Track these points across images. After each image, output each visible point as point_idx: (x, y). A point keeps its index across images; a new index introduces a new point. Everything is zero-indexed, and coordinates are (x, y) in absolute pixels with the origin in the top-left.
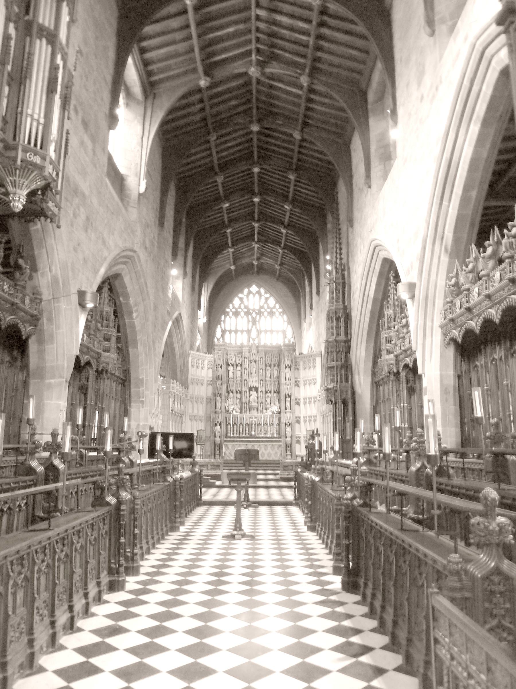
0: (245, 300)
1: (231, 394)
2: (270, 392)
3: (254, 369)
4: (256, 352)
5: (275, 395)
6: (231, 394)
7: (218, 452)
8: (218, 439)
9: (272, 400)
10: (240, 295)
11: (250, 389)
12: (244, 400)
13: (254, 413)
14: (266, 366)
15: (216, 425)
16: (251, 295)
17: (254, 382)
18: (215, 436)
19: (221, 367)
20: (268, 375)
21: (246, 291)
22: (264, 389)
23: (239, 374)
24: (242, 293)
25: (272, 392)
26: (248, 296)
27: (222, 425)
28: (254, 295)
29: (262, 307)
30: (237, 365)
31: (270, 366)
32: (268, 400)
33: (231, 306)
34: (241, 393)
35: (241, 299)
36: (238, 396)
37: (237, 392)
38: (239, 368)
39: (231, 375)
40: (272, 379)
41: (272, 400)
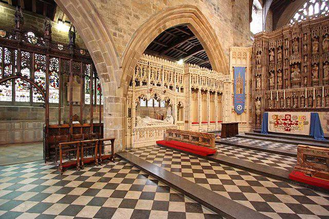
0: (305, 13)
1: (273, 75)
2: (318, 65)
3: (297, 47)
4: (298, 31)
5: (325, 67)
6: (273, 75)
7: (258, 121)
8: (258, 111)
9: (321, 73)
10: (300, 10)
11: (292, 66)
12: (285, 77)
13: (297, 88)
14: (312, 40)
15: (257, 100)
16: (311, 7)
17: (294, 59)
18: (256, 109)
19: (260, 54)
20: (315, 48)
21: (305, 5)
22: (308, 63)
23: (280, 55)
24: (302, 7)
25: (321, 65)
26: (307, 8)
27: (262, 100)
28: (314, 5)
29: (323, 11)
30: (278, 49)
31: (318, 38)
32: (315, 74)
33: (292, 21)
34: (282, 71)
35: (301, 13)
36: (280, 75)
37: (278, 72)
38: (280, 51)
39: (271, 58)
40: (321, 52)
41: (321, 73)
